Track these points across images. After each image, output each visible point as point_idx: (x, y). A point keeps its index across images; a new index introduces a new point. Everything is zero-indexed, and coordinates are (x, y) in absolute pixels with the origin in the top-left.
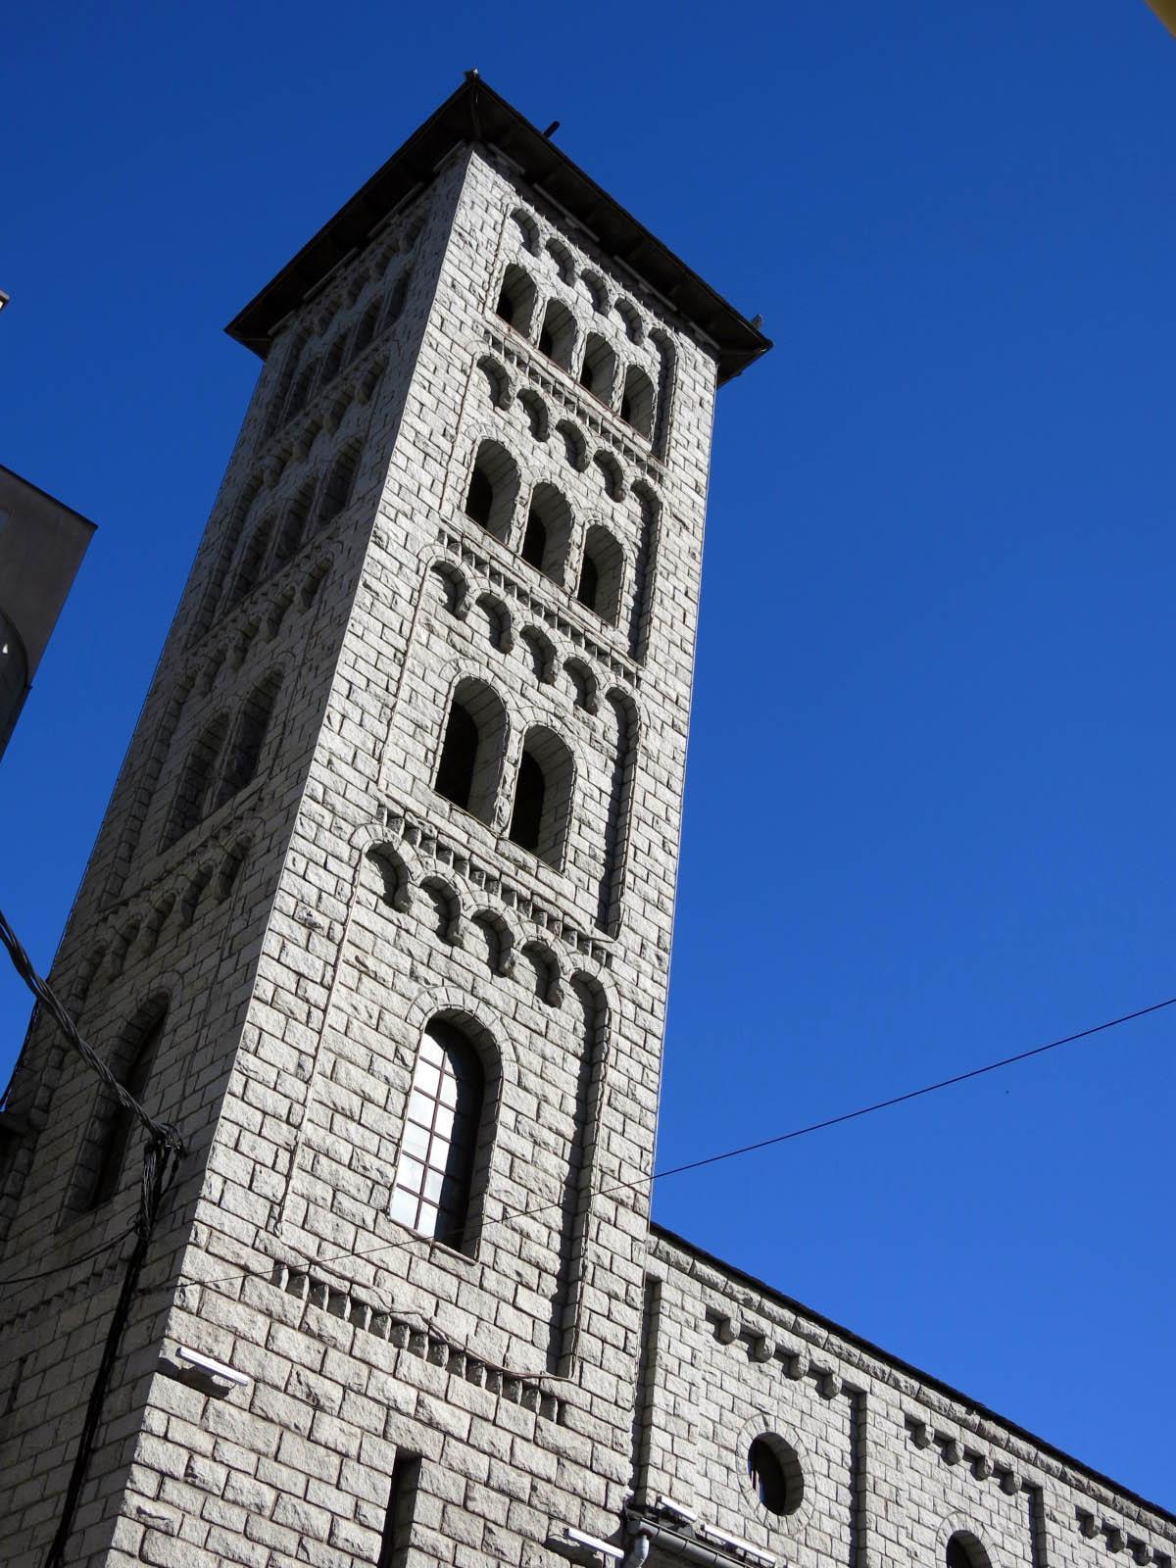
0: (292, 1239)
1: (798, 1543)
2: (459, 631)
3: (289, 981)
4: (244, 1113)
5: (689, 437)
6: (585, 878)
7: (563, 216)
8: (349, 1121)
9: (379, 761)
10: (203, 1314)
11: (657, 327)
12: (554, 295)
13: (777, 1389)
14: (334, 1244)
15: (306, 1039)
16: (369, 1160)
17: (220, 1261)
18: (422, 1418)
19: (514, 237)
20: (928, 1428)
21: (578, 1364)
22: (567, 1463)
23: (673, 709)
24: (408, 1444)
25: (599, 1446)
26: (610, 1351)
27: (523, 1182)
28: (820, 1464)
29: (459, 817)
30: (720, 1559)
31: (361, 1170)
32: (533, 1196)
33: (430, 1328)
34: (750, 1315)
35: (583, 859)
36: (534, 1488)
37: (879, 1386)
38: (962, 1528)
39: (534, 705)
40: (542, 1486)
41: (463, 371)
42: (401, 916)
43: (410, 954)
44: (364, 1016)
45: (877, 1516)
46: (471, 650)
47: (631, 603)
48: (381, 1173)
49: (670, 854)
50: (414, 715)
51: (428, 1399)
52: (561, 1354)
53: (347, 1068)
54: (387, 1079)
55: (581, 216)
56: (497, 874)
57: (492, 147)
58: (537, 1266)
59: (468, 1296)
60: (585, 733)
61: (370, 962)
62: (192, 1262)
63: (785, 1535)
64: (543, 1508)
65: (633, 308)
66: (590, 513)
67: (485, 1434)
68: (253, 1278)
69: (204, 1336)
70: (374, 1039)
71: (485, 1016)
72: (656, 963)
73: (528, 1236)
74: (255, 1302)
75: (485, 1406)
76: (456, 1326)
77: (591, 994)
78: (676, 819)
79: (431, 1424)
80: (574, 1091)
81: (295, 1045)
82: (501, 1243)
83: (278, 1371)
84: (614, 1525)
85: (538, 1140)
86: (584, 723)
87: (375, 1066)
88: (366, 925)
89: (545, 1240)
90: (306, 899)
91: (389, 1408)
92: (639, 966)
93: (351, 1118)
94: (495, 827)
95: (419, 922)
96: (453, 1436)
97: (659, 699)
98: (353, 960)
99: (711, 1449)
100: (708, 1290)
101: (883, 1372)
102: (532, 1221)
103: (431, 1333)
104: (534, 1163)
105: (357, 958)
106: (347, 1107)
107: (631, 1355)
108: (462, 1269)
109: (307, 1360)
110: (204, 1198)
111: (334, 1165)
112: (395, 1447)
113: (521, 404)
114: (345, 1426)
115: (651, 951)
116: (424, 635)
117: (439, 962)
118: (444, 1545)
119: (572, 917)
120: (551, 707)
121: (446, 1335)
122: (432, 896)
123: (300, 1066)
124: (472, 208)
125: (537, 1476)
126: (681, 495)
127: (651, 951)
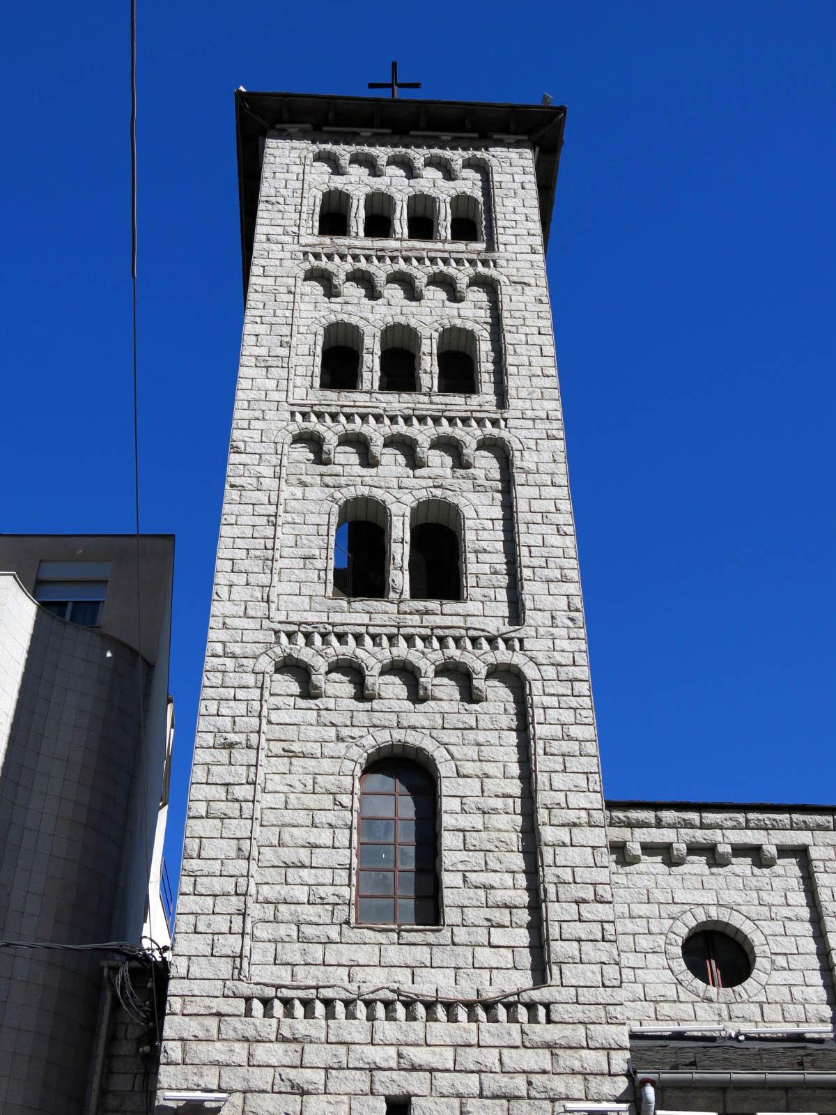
0: (264, 973)
2: (330, 472)
3: (220, 793)
4: (197, 903)
6: (491, 592)
7: (358, 134)
8: (301, 870)
9: (268, 602)
10: (188, 1061)
11: (467, 156)
12: (368, 190)
14: (306, 964)
15: (239, 828)
16: (322, 891)
17: (194, 1018)
18: (405, 1066)
19: (322, 173)
21: (555, 969)
22: (559, 1052)
23: (547, 425)
24: (394, 1090)
25: (591, 1027)
26: (587, 947)
27: (478, 848)
29: (358, 605)
30: (734, 1076)
31: (319, 901)
33: (399, 995)
35: (484, 580)
36: (530, 1083)
39: (411, 489)
40: (536, 1079)
41: (290, 292)
42: (318, 701)
43: (333, 725)
44: (300, 787)
46: (343, 480)
47: (491, 367)
48: (337, 896)
49: (566, 534)
50: (301, 552)
51: (405, 1050)
52: (540, 971)
53: (290, 832)
54: (330, 825)
55: (368, 124)
56: (395, 630)
57: (278, 126)
58: (506, 906)
59: (440, 956)
60: (468, 485)
61: (296, 747)
62: (171, 1028)
64: (543, 1095)
65: (440, 157)
66: (437, 325)
67: (469, 1058)
68: (226, 1018)
69: (190, 1077)
70: (310, 801)
71: (413, 739)
72: (570, 624)
73: (492, 887)
74: (232, 1034)
75: (464, 1035)
76: (427, 986)
77: (512, 677)
78: (566, 506)
79: (414, 1068)
80: (515, 757)
81: (233, 836)
82: (466, 903)
83: (262, 1078)
84: (622, 1084)
85: (486, 810)
86: (464, 478)
87: (317, 820)
88: (288, 722)
89: (510, 883)
90: (222, 729)
91: (371, 1070)
92: (553, 634)
93: (304, 866)
94: (392, 595)
95: (336, 697)
96: (438, 1070)
97: (530, 423)
102: (492, 874)
103: (401, 998)
104: (486, 829)
105: (284, 750)
106: (295, 860)
107: (610, 941)
108: (431, 938)
109: (287, 1061)
110: (174, 978)
111: (293, 907)
112: (383, 1098)
113: (354, 284)
114: (331, 1098)
115: (562, 618)
116: (298, 492)
117: (362, 718)
119: (475, 629)
120: (430, 483)
121: (416, 995)
122: (343, 674)
123: (240, 849)
124: (274, 178)
125: (531, 1072)
126: (518, 264)
127: (562, 618)
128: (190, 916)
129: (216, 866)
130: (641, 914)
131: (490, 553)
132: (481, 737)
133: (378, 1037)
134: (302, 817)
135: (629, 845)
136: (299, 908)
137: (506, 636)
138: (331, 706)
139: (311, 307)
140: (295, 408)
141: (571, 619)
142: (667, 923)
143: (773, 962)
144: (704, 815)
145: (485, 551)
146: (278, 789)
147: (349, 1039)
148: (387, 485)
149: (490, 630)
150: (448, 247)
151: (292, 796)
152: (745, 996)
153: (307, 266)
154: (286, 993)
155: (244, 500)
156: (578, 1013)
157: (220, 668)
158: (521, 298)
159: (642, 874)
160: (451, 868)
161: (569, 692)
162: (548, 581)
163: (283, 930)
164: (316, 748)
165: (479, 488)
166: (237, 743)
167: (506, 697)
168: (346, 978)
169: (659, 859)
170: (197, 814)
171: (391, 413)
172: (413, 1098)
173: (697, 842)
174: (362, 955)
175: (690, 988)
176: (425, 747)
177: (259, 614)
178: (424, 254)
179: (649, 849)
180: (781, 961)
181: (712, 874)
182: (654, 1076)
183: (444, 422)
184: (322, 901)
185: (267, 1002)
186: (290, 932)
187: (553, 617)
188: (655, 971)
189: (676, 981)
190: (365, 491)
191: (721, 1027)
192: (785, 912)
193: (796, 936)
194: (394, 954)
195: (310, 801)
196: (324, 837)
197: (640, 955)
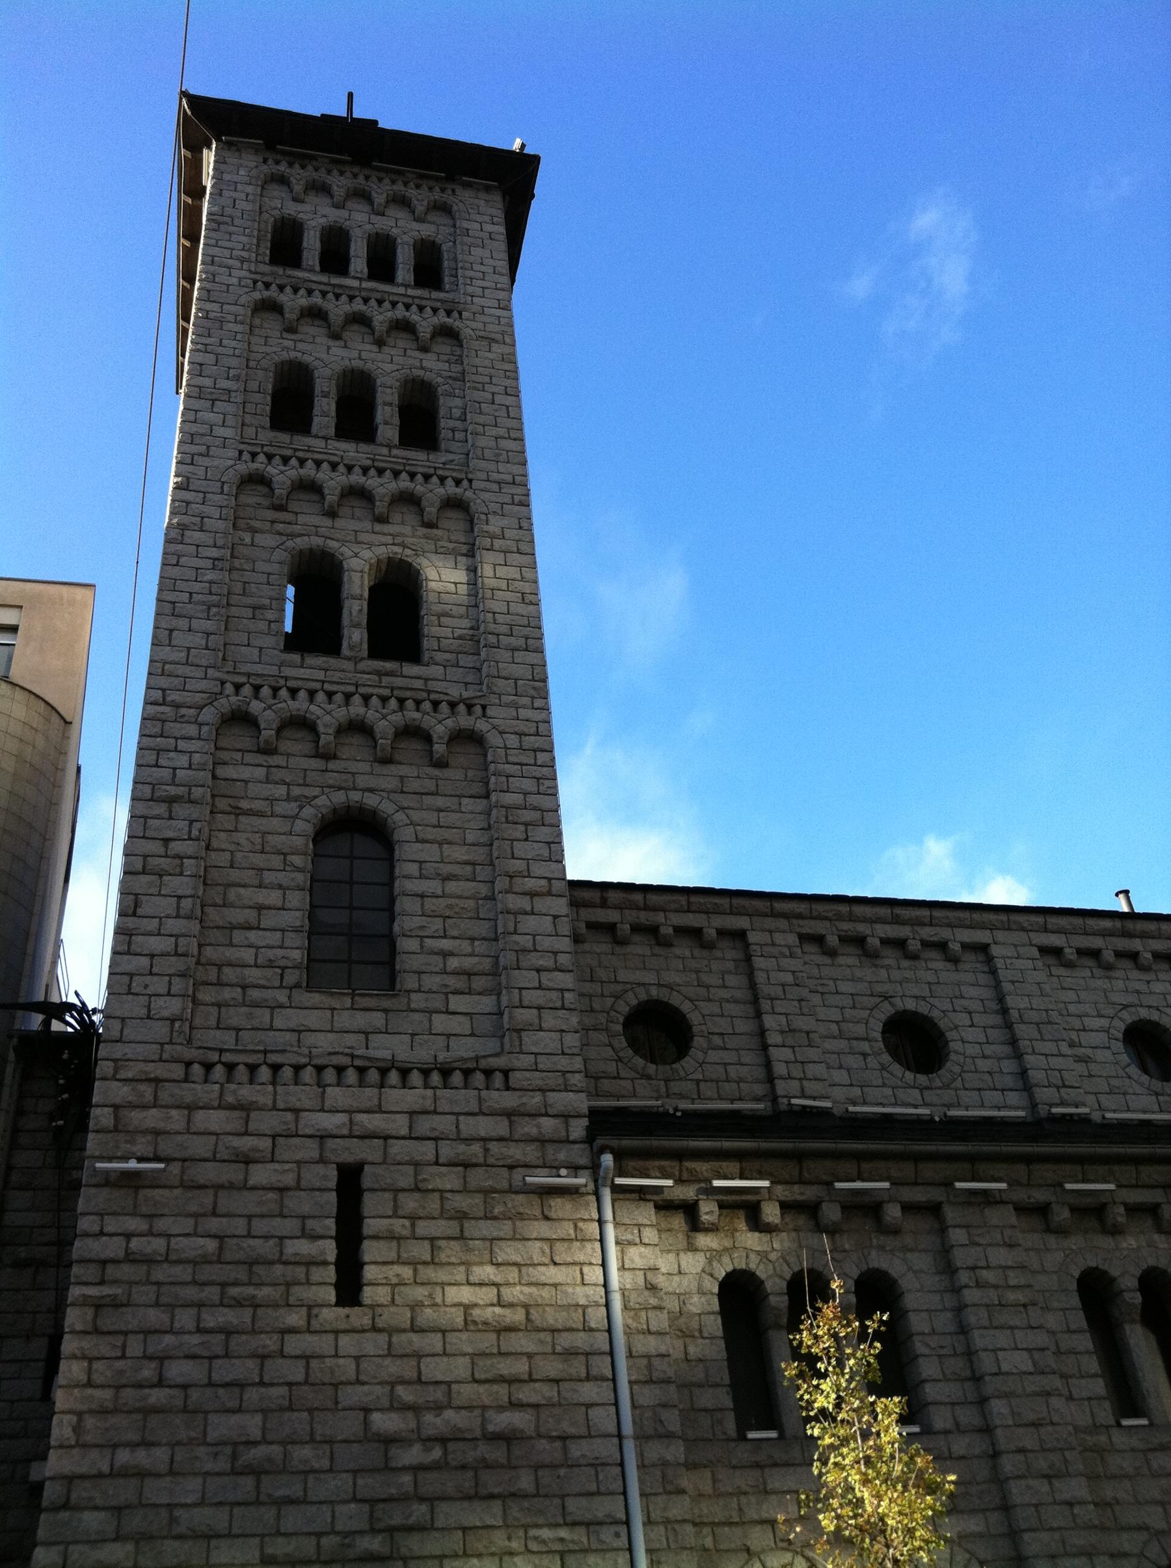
1: (956, 1089)
2: (282, 519)
5: (483, 268)
13: (896, 975)
20: (1067, 950)
24: (347, 1158)
28: (962, 1019)
29: (311, 660)
34: (845, 926)
36: (486, 1150)
37: (1000, 935)
38: (1136, 1019)
45: (1031, 1040)
46: (297, 529)
50: (249, 601)
61: (244, 804)
63: (940, 1088)
67: (425, 1125)
70: (259, 860)
83: (200, 1146)
97: (495, 487)
99: (842, 1044)
100: (795, 921)
101: (1002, 922)
108: (386, 1003)
111: (239, 970)
114: (276, 1166)
118: (400, 1226)
120: (389, 539)
129: (152, 925)
133: (328, 1104)
134: (249, 876)
136: (247, 971)
139: (262, 341)
140: (242, 447)
142: (609, 1001)
143: (709, 1041)
146: (223, 847)
147: (298, 1105)
150: (410, 292)
151: (239, 855)
152: (682, 1074)
153: (257, 295)
154: (228, 1057)
155: (187, 540)
156: (537, 1079)
158: (488, 355)
161: (532, 762)
162: (514, 650)
163: (227, 994)
165: (442, 550)
168: (295, 1044)
172: (367, 1168)
174: (313, 1019)
177: (204, 662)
178: (386, 296)
180: (717, 1041)
181: (654, 955)
182: (614, 1143)
183: (404, 475)
185: (208, 1067)
190: (316, 541)
191: (659, 1103)
192: (723, 994)
193: (732, 1017)
194: (345, 1019)
195: (259, 860)
196: (273, 897)
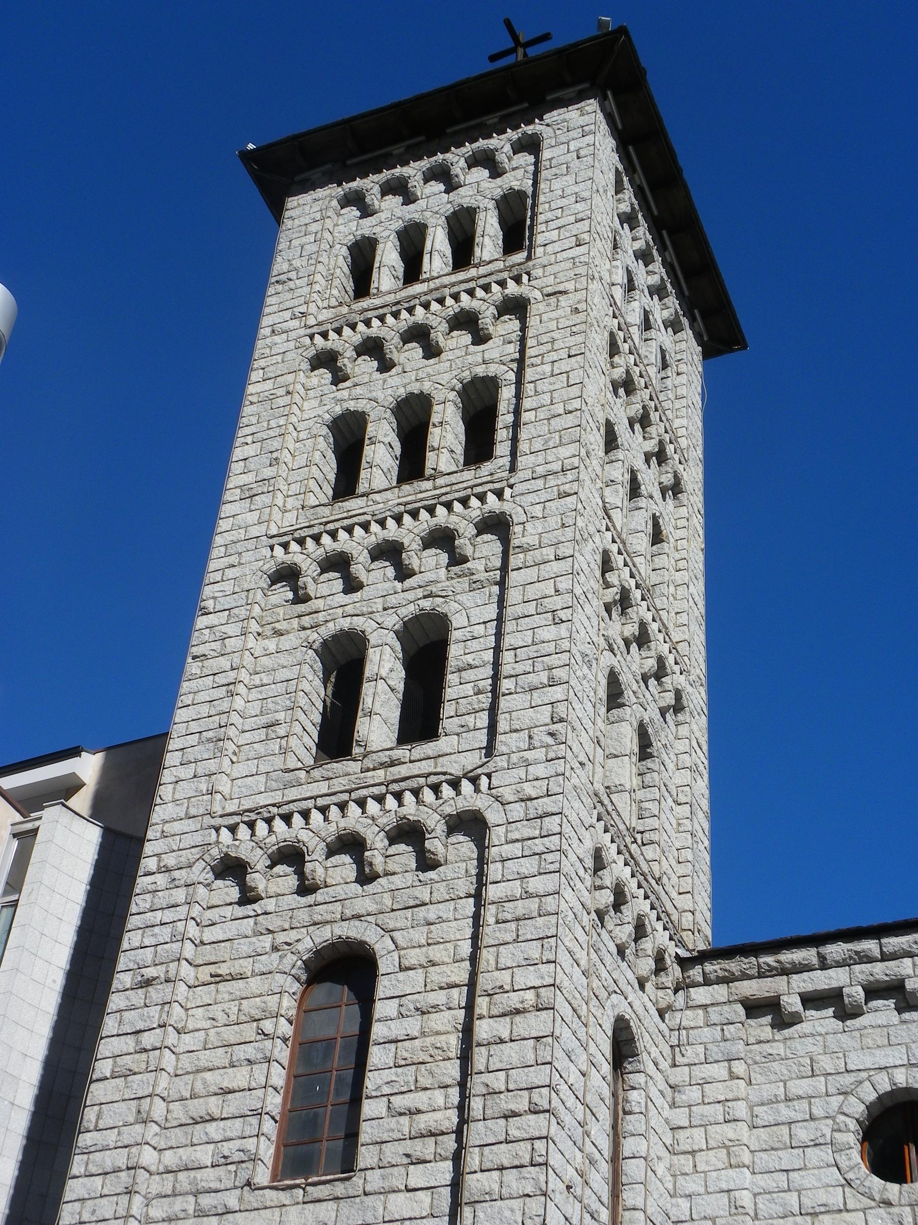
31: (223, 1160)
32: (422, 1067)
42: (255, 906)
46: (321, 617)
48: (243, 1151)
49: (563, 622)
54: (249, 1061)
72: (550, 740)
81: (134, 1096)
86: (459, 576)
88: (221, 939)
90: (141, 963)
93: (213, 1119)
94: (356, 750)
98: (209, 979)
106: (203, 1113)
111: (192, 1174)
120: (420, 593)
128: (76, 1204)
130: (801, 1093)
131: (477, 667)
132: (431, 913)
135: (784, 999)
136: (199, 1174)
137: (472, 774)
138: (270, 908)
141: (552, 734)
142: (836, 1101)
144: (884, 941)
145: (471, 667)
146: (199, 1026)
148: (370, 610)
149: (453, 772)
157: (150, 888)
159: (806, 1036)
160: (374, 1094)
164: (246, 966)
165: (474, 585)
166: (154, 979)
167: (469, 854)
169: (830, 1011)
170: (101, 1076)
171: (380, 516)
173: (877, 981)
175: (861, 1189)
176: (368, 940)
179: (812, 1000)
181: (903, 1022)
184: (226, 1161)
186: (185, 1206)
187: (530, 737)
188: (816, 1172)
189: (844, 1182)
197: (796, 1151)
